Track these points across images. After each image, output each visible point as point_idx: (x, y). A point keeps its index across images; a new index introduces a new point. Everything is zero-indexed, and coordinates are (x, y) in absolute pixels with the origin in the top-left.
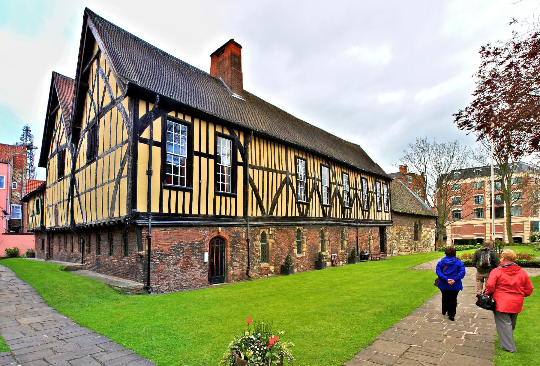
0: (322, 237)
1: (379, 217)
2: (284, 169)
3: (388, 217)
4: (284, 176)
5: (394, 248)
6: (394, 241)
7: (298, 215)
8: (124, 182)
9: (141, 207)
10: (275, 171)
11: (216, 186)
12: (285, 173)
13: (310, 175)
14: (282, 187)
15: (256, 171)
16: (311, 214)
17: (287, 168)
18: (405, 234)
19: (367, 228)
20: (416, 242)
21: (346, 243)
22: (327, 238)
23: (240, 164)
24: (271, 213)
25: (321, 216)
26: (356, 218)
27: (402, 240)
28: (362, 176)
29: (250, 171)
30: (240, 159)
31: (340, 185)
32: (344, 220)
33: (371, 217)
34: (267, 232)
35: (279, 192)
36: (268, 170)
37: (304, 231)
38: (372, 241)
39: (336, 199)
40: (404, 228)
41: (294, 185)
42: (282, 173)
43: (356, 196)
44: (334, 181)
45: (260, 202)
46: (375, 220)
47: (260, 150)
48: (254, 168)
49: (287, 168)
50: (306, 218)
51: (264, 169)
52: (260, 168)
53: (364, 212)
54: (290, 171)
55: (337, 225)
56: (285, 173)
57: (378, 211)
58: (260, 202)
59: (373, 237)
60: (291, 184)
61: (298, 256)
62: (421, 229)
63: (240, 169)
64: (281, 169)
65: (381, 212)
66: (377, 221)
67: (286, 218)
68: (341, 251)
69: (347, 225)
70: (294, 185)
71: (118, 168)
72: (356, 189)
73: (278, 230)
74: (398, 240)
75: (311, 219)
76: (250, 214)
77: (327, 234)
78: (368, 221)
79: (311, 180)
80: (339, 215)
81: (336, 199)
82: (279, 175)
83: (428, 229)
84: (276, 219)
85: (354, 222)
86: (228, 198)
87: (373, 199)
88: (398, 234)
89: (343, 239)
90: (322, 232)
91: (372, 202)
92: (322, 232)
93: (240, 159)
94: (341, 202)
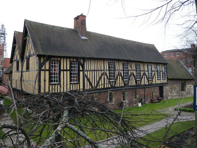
0: (124, 94)
1: (158, 82)
2: (103, 69)
3: (165, 81)
4: (102, 72)
5: (169, 96)
7: (110, 86)
8: (37, 83)
9: (42, 91)
10: (99, 70)
11: (71, 80)
12: (103, 70)
13: (116, 69)
14: (101, 76)
15: (89, 72)
17: (104, 68)
18: (176, 88)
20: (183, 92)
21: (138, 96)
22: (126, 95)
23: (81, 71)
24: (97, 87)
25: (123, 85)
26: (144, 84)
28: (148, 64)
29: (86, 73)
30: (81, 69)
31: (134, 70)
32: (137, 85)
34: (94, 95)
35: (100, 78)
36: (94, 71)
37: (113, 93)
38: (154, 94)
39: (132, 77)
40: (175, 86)
41: (108, 75)
42: (101, 71)
43: (144, 74)
44: (131, 69)
45: (91, 84)
46: (156, 84)
47: (90, 64)
48: (87, 71)
49: (104, 68)
51: (92, 71)
52: (90, 71)
53: (149, 81)
54: (106, 69)
55: (132, 88)
56: (103, 70)
58: (91, 84)
59: (155, 92)
60: (106, 74)
62: (186, 85)
63: (81, 73)
64: (101, 69)
65: (161, 79)
66: (158, 84)
67: (104, 88)
68: (135, 100)
70: (108, 75)
71: (35, 78)
72: (144, 71)
73: (99, 94)
74: (171, 92)
75: (118, 87)
76: (86, 88)
77: (127, 93)
78: (152, 84)
79: (117, 71)
80: (134, 83)
81: (132, 77)
82: (100, 72)
83: (190, 85)
84: (99, 89)
85: (143, 86)
86: (76, 85)
87: (155, 74)
88: (171, 89)
89: (136, 94)
90: (124, 92)
91: (154, 75)
92: (124, 92)
93: (81, 69)
94: (135, 77)
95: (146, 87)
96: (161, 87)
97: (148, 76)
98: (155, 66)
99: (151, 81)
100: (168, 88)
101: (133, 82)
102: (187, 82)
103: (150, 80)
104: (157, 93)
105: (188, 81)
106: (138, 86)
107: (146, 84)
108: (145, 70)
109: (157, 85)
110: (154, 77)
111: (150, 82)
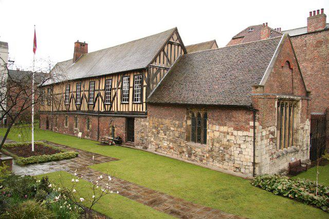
1: (123, 108)
3: (142, 108)
6: (150, 134)
16: (71, 109)
18: (168, 129)
19: (109, 118)
27: (162, 135)
32: (89, 112)
33: (114, 109)
40: (167, 122)
50: (69, 111)
53: (106, 106)
57: (123, 104)
61: (66, 127)
65: (128, 104)
66: (122, 113)
69: (90, 115)
72: (99, 90)
78: (110, 112)
80: (86, 109)
85: (96, 113)
88: (155, 128)
95: (101, 116)
96: (130, 120)
97: (104, 98)
98: (118, 79)
99: (109, 106)
100: (147, 124)
101: (84, 107)
102: (209, 114)
103: (108, 105)
104: (121, 131)
105: (216, 113)
106: (90, 113)
107: (100, 110)
108: (101, 89)
109: (120, 114)
110: (114, 99)
111: (108, 108)
